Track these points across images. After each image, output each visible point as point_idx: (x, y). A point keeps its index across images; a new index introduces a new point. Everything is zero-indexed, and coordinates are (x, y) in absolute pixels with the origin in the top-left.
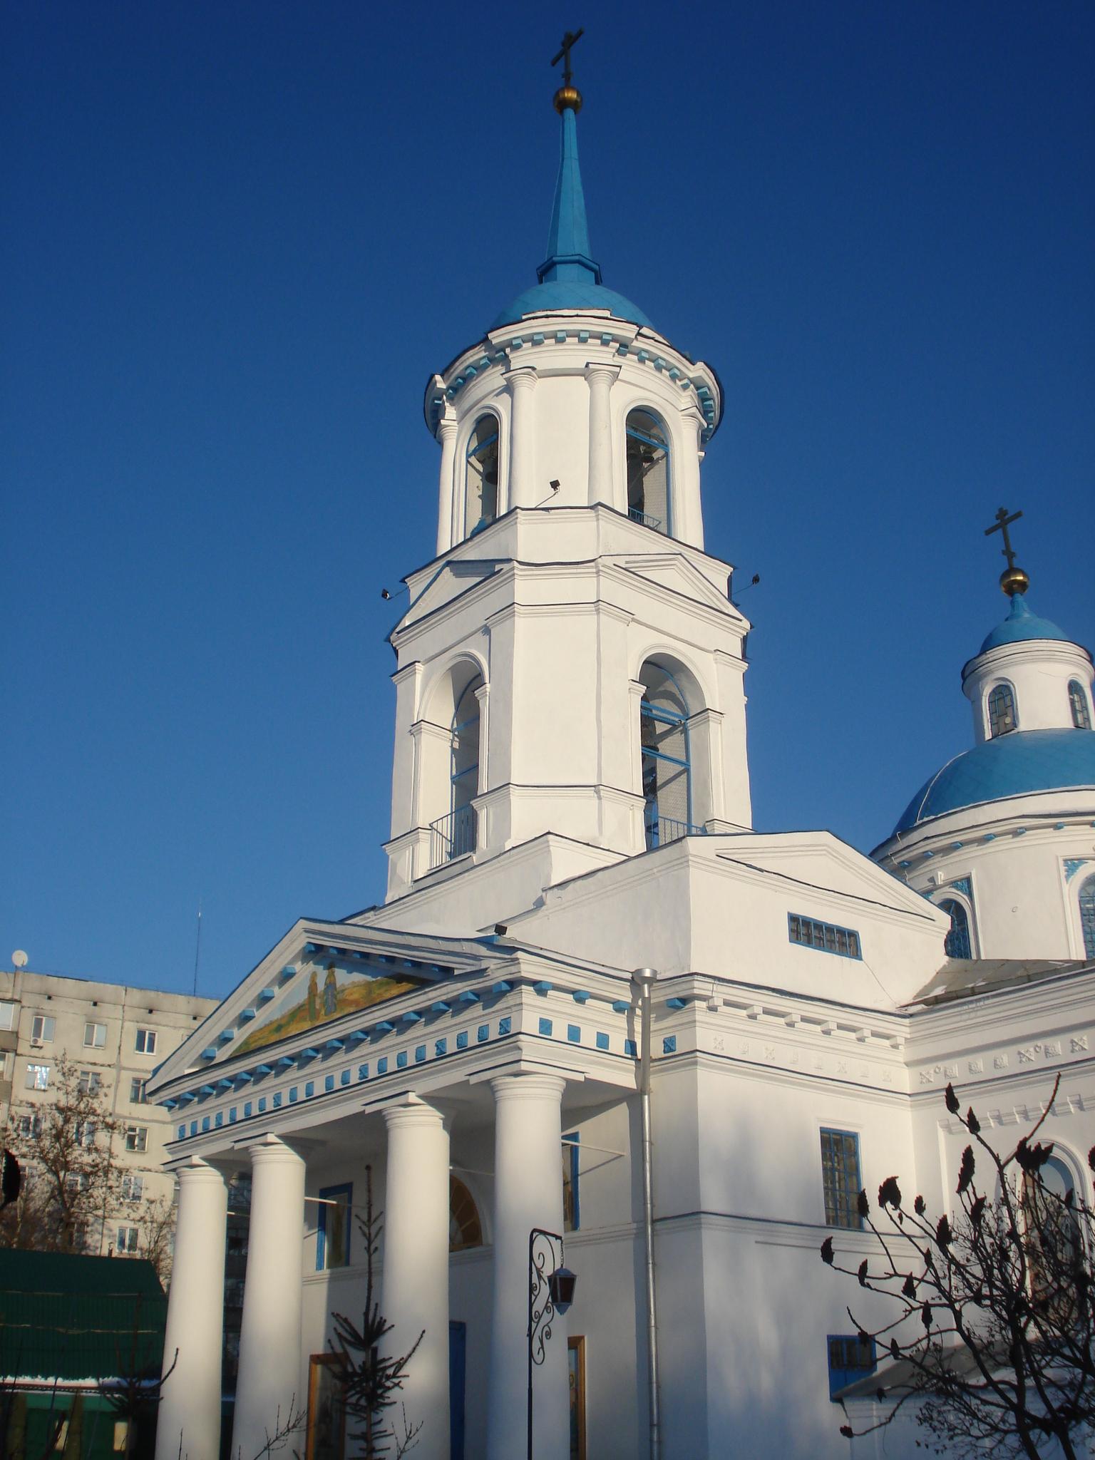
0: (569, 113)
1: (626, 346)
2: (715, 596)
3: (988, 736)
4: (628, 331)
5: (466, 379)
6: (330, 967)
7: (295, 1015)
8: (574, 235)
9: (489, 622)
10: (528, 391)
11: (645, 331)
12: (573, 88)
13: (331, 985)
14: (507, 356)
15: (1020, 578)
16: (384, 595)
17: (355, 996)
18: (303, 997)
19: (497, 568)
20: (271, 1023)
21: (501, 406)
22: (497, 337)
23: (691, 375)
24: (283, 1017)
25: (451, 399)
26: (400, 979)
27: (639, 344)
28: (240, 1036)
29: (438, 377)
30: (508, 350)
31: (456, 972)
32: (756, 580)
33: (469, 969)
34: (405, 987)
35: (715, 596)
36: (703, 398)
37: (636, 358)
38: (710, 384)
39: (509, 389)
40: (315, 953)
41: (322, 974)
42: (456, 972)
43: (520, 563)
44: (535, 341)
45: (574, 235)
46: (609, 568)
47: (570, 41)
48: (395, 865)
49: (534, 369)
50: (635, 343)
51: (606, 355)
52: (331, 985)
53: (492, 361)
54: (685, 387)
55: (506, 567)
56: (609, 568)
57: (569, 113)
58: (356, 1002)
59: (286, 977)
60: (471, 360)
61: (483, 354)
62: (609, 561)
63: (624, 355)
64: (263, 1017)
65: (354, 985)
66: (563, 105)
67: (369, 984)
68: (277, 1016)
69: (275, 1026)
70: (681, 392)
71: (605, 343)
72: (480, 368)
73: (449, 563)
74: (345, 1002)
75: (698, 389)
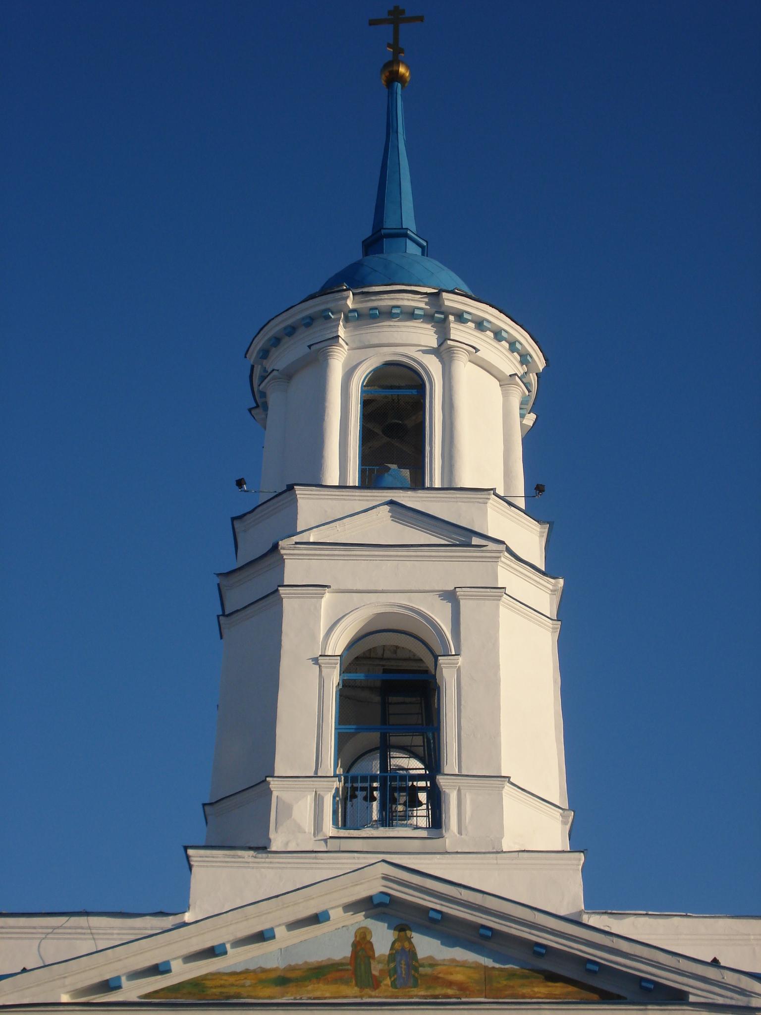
5: (389, 314)
6: (401, 928)
7: (320, 972)
9: (459, 592)
10: (464, 370)
12: (408, 67)
13: (403, 953)
14: (445, 320)
16: (240, 483)
17: (459, 977)
18: (342, 951)
19: (475, 541)
20: (264, 971)
21: (433, 366)
22: (451, 301)
24: (292, 968)
25: (347, 320)
26: (551, 977)
28: (181, 972)
30: (451, 318)
31: (692, 999)
33: (720, 1001)
34: (558, 988)
39: (444, 351)
40: (375, 906)
42: (692, 999)
43: (509, 550)
44: (480, 325)
47: (396, 17)
48: (289, 809)
49: (477, 350)
52: (403, 953)
53: (428, 318)
55: (492, 546)
58: (463, 988)
59: (316, 919)
60: (406, 303)
61: (423, 305)
64: (236, 959)
65: (454, 962)
66: (394, 77)
67: (486, 967)
68: (270, 965)
69: (273, 975)
72: (411, 315)
73: (391, 503)
74: (435, 980)
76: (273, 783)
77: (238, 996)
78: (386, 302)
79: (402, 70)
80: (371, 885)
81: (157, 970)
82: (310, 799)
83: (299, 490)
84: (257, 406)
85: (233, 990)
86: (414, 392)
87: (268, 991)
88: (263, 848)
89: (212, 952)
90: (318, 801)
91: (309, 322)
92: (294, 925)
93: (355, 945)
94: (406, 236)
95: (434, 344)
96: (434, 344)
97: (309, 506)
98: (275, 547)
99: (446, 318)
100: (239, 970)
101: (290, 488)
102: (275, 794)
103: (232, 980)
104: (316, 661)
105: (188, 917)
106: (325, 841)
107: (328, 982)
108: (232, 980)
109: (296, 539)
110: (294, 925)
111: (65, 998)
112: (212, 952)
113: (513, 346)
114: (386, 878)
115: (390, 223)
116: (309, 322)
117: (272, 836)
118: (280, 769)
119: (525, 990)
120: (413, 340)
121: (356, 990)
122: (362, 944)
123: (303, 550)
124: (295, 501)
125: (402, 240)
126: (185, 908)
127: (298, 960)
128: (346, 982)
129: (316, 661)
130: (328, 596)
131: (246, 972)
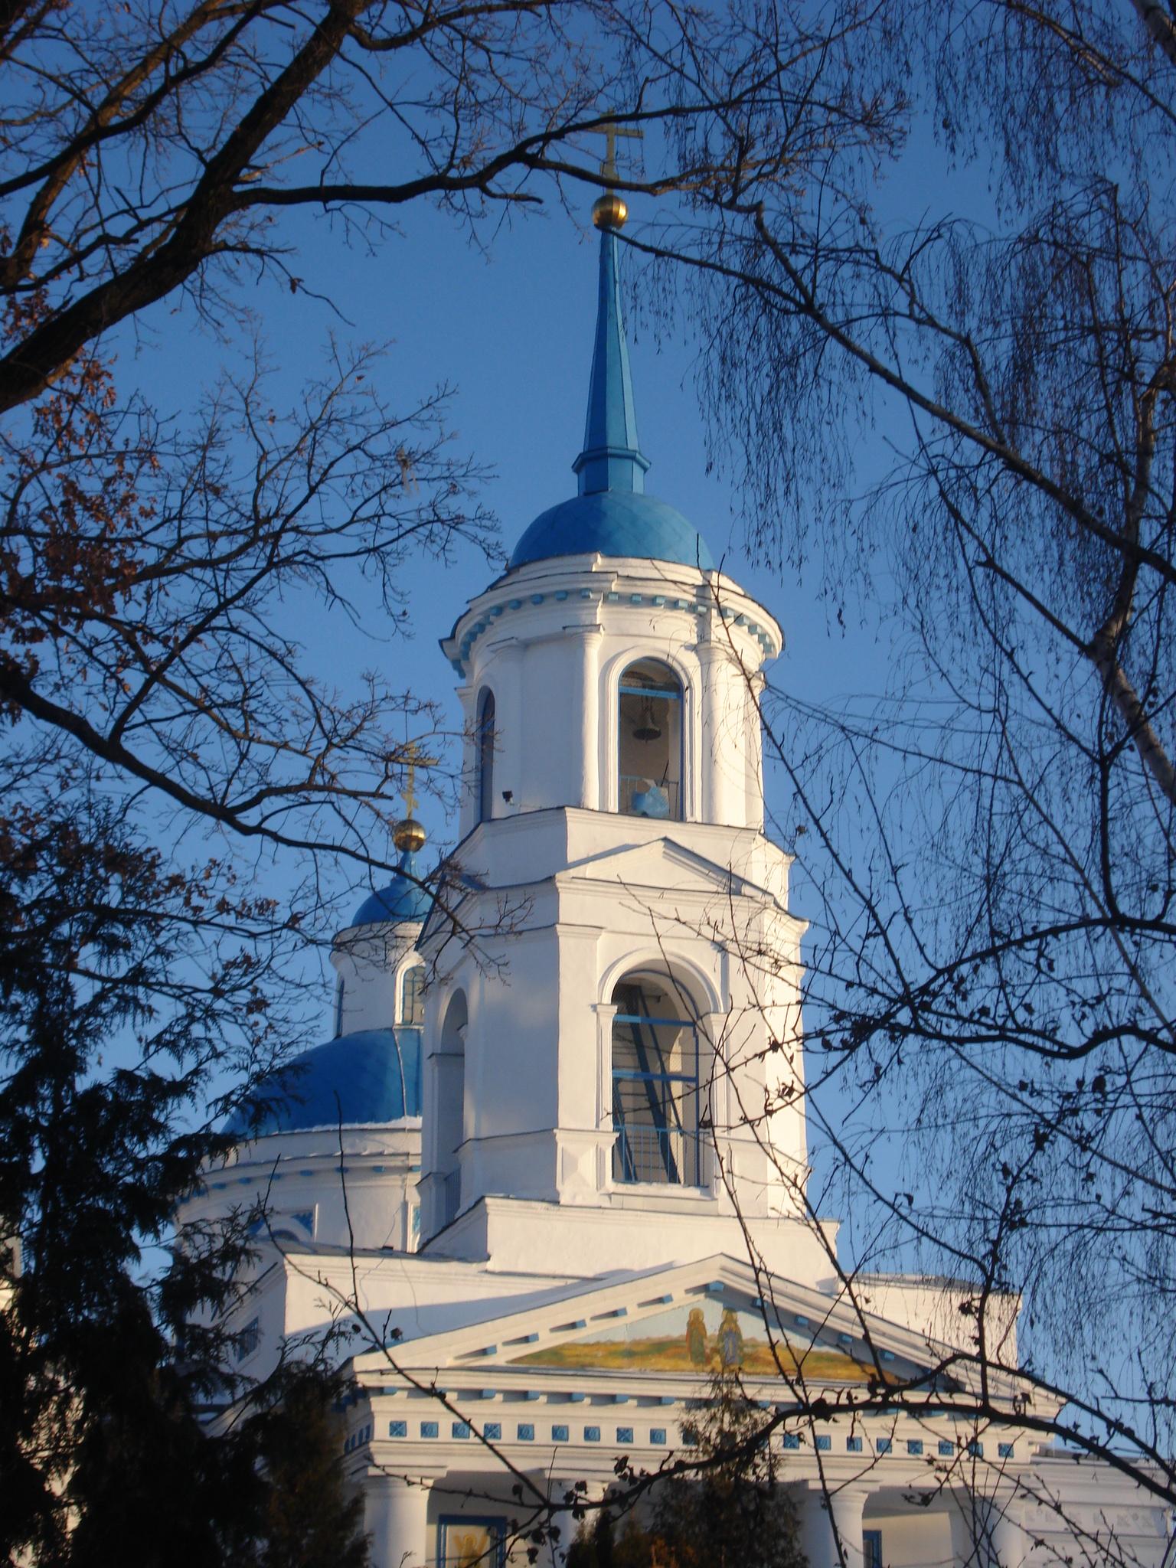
3: (398, 1019)
5: (652, 601)
6: (730, 1309)
7: (660, 1348)
13: (730, 1332)
15: (421, 835)
18: (677, 1329)
20: (613, 1344)
24: (637, 1343)
25: (606, 599)
41: (713, 1315)
48: (574, 1163)
52: (730, 1332)
53: (692, 608)
68: (618, 1338)
72: (674, 604)
73: (665, 839)
76: (560, 1136)
77: (592, 1365)
78: (651, 590)
79: (622, 212)
80: (710, 1276)
81: (526, 1340)
82: (592, 1152)
83: (570, 813)
84: (453, 637)
85: (588, 1360)
86: (671, 696)
87: (618, 1362)
88: (556, 1202)
89: (573, 1326)
90: (600, 1154)
91: (564, 596)
92: (641, 1305)
93: (690, 1324)
94: (633, 458)
95: (695, 641)
96: (695, 641)
97: (583, 832)
98: (551, 879)
99: (709, 610)
100: (592, 1341)
101: (561, 808)
102: (560, 1146)
103: (586, 1350)
104: (594, 1007)
105: (490, 1265)
106: (610, 1195)
107: (668, 1357)
108: (586, 1350)
109: (572, 872)
110: (641, 1305)
111: (450, 1362)
112: (573, 1326)
113: (762, 638)
114: (723, 1269)
115: (613, 440)
116: (564, 596)
117: (559, 1186)
118: (564, 1120)
119: (831, 1372)
120: (670, 636)
121: (690, 1365)
122: (696, 1324)
123: (580, 885)
124: (564, 823)
125: (628, 462)
126: (488, 1258)
127: (641, 1335)
128: (684, 1358)
129: (594, 1007)
130: (604, 936)
131: (597, 1344)
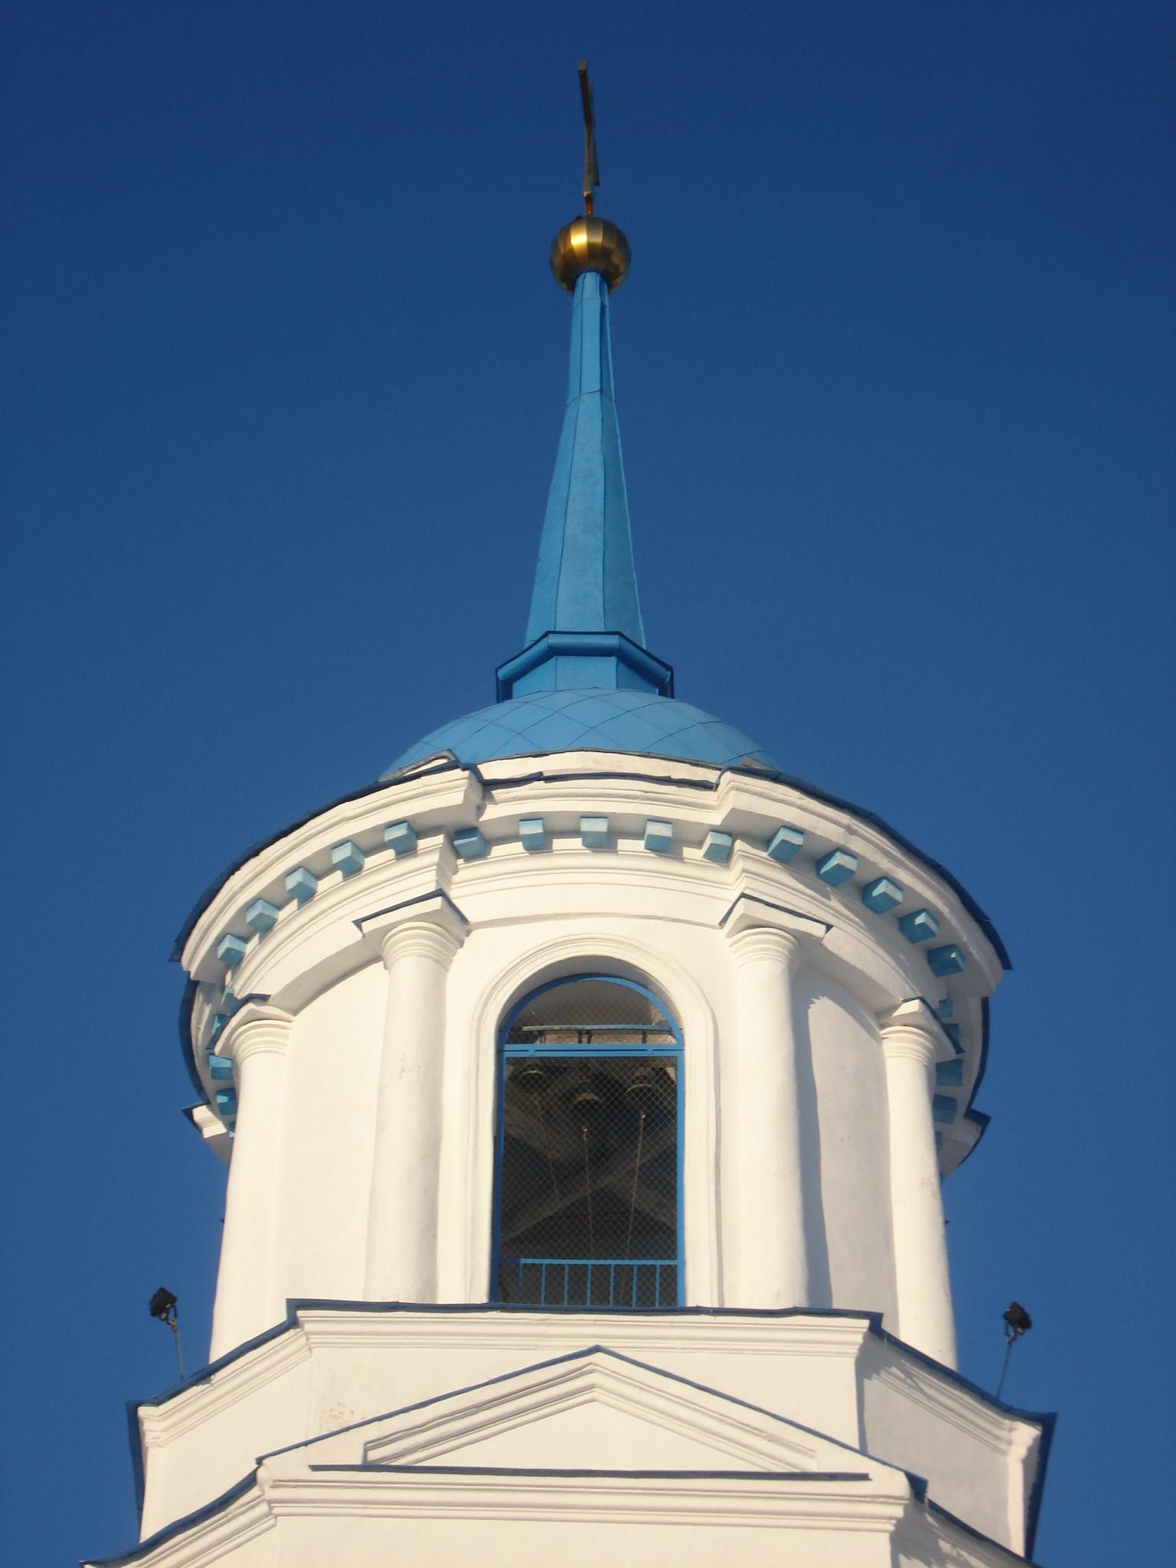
0: (589, 283)
1: (469, 831)
2: (757, 1432)
4: (442, 792)
8: (574, 584)
11: (491, 770)
22: (194, 957)
23: (716, 819)
27: (501, 809)
29: (201, 1113)
32: (1018, 1319)
35: (757, 1432)
36: (809, 861)
37: (518, 847)
38: (789, 815)
45: (574, 584)
46: (297, 1483)
49: (263, 999)
50: (491, 812)
51: (420, 872)
54: (721, 856)
56: (297, 1483)
57: (589, 283)
61: (207, 1010)
62: (295, 1465)
63: (480, 854)
70: (715, 873)
71: (405, 849)
75: (764, 842)
